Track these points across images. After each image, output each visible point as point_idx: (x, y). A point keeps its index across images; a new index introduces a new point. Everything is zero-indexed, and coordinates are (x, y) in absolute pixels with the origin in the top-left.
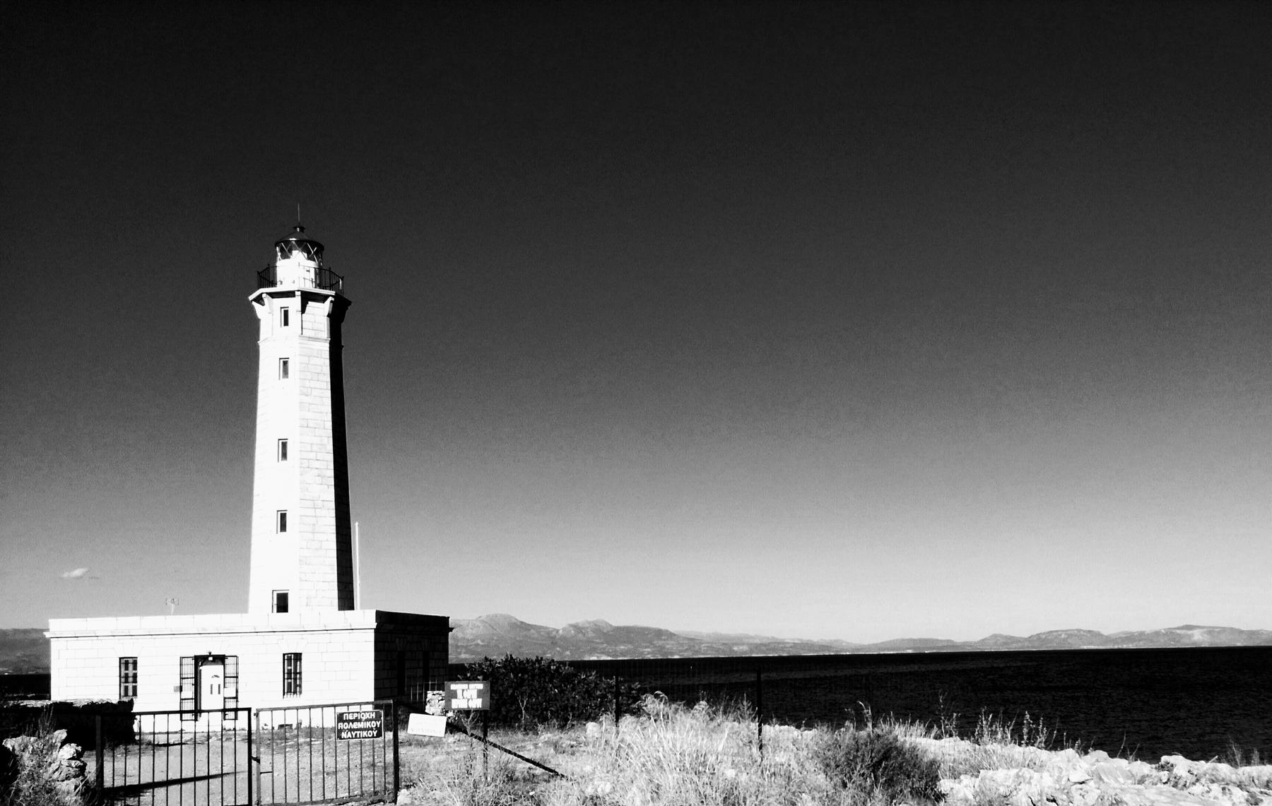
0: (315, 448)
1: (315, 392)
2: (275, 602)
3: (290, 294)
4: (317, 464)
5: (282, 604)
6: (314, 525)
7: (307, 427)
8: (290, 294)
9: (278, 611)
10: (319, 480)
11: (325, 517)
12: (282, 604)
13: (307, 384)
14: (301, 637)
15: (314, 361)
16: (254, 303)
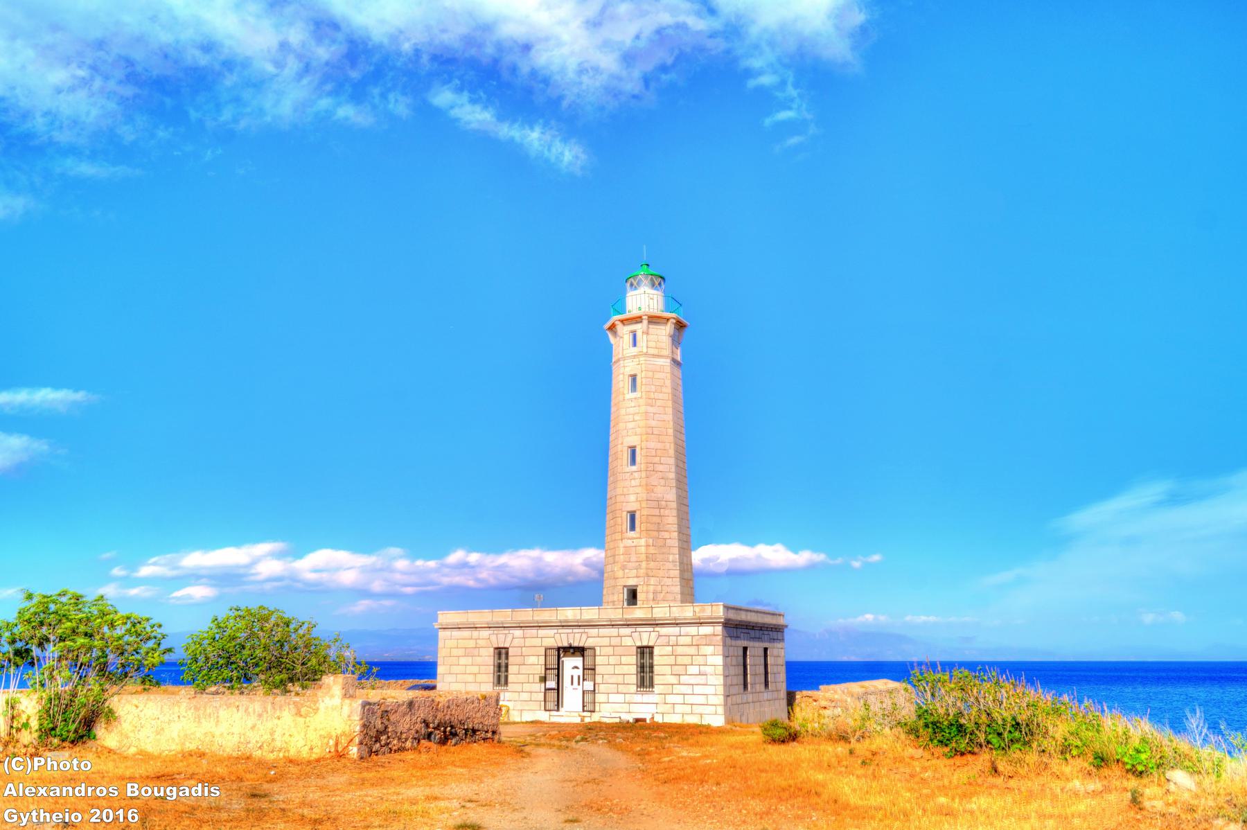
0: (659, 453)
1: (659, 403)
2: (626, 597)
3: (637, 320)
4: (660, 468)
5: (633, 596)
6: (658, 523)
7: (652, 434)
8: (637, 320)
9: (629, 604)
10: (662, 482)
11: (668, 516)
12: (633, 596)
13: (652, 396)
14: (652, 629)
15: (657, 375)
16: (607, 332)
